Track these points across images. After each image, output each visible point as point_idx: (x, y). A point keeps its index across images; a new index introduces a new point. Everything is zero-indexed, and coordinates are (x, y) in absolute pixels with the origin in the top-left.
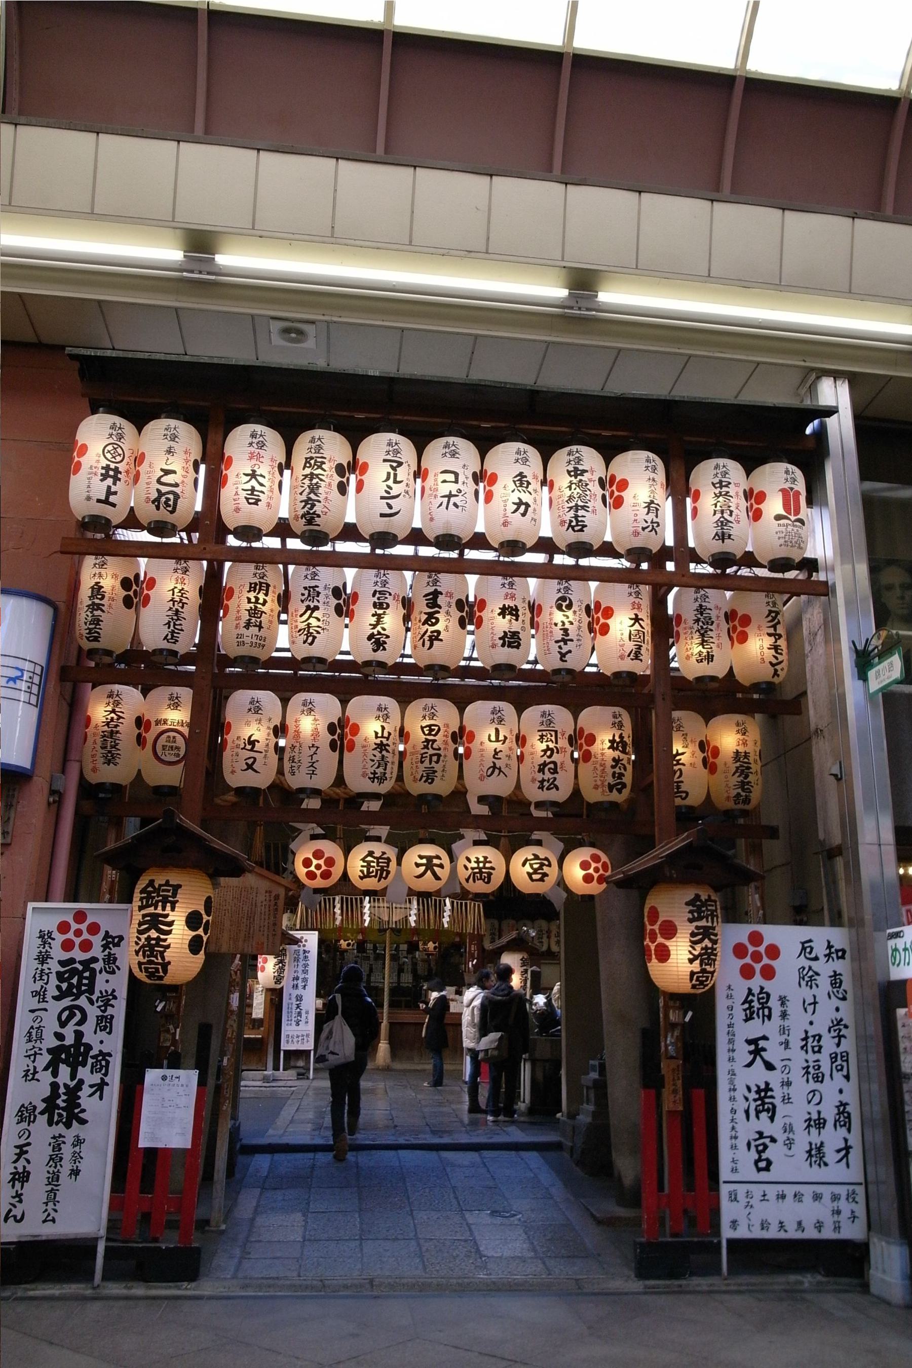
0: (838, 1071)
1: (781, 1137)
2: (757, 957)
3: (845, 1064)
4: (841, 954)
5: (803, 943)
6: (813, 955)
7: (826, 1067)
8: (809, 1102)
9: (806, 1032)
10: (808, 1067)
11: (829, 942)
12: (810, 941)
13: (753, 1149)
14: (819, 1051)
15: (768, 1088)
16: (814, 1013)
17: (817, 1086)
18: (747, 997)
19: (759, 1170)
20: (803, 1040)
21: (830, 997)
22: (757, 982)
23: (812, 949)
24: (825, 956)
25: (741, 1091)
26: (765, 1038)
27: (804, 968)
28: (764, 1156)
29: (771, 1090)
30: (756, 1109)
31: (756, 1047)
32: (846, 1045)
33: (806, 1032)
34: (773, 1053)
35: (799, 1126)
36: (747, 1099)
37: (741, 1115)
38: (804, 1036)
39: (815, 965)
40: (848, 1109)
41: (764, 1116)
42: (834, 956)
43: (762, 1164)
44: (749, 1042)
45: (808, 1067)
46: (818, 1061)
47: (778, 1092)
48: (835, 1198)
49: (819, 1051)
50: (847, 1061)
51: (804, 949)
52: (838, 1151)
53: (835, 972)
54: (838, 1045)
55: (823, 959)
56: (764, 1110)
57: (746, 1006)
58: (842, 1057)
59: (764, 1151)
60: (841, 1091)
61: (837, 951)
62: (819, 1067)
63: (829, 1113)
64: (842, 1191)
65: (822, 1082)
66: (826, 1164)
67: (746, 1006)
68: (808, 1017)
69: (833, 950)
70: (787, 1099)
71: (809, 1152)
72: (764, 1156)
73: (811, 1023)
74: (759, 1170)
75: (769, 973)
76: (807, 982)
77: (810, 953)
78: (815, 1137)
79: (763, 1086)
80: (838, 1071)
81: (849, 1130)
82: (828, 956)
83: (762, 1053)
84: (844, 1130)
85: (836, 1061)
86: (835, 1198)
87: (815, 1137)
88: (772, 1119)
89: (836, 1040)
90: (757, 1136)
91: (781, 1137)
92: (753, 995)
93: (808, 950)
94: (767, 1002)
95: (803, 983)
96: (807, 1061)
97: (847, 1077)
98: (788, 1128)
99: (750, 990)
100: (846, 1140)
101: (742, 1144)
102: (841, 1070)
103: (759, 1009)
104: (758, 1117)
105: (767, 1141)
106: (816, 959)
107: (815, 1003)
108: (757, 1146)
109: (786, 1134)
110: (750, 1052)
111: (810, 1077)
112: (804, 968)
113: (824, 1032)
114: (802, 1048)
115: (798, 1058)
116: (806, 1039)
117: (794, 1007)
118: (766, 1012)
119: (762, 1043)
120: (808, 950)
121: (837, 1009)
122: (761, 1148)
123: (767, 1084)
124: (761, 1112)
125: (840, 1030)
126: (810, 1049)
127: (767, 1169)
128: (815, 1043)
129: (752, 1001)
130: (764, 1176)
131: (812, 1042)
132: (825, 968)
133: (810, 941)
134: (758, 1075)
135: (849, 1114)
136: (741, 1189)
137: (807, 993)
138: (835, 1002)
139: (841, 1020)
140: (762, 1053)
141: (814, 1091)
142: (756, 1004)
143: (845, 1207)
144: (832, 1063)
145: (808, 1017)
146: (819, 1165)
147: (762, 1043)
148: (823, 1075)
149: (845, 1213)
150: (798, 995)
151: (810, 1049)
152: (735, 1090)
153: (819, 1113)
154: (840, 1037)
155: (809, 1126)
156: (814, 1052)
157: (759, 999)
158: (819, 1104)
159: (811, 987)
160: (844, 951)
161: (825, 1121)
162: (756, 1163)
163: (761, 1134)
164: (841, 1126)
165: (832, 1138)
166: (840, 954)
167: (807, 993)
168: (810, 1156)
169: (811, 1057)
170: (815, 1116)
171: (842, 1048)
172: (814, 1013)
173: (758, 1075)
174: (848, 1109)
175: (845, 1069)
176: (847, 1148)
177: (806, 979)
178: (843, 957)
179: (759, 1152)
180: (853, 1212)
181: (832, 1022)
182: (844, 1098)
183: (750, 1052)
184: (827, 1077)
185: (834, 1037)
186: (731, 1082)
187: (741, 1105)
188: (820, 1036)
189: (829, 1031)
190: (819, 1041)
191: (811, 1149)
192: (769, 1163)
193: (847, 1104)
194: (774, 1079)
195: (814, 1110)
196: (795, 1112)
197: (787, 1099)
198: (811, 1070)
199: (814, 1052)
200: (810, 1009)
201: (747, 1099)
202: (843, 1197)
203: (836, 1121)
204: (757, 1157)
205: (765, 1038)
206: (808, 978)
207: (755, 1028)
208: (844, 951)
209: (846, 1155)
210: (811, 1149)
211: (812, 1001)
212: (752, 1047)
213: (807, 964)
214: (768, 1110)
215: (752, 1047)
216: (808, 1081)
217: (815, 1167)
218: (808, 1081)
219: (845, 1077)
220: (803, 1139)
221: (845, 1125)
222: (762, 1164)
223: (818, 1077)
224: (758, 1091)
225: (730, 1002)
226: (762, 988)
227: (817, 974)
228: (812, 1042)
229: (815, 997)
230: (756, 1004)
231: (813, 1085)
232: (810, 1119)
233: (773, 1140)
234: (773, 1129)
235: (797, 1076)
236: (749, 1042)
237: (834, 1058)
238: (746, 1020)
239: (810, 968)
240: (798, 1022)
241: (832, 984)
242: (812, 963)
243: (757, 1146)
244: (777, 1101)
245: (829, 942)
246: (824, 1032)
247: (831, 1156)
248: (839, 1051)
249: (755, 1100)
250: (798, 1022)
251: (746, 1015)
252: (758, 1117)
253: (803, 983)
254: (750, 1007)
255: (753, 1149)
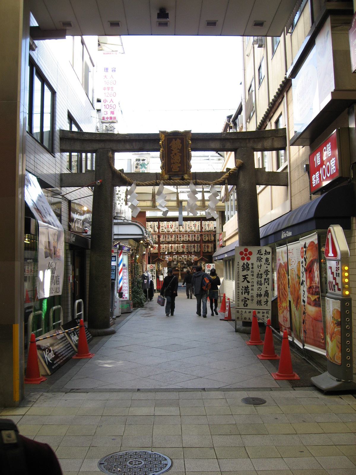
0: (266, 283)
1: (250, 298)
2: (246, 255)
3: (268, 281)
4: (269, 253)
5: (258, 251)
6: (261, 254)
7: (263, 282)
8: (258, 290)
9: (258, 273)
10: (258, 282)
11: (266, 250)
12: (261, 250)
13: (243, 301)
14: (261, 278)
15: (248, 287)
16: (260, 268)
17: (260, 286)
18: (243, 265)
19: (245, 306)
20: (257, 275)
21: (265, 264)
22: (245, 261)
23: (261, 252)
24: (264, 254)
25: (241, 287)
26: (247, 275)
27: (258, 257)
28: (246, 303)
29: (249, 288)
30: (244, 292)
31: (245, 277)
32: (268, 276)
33: (258, 273)
34: (249, 278)
35: (255, 296)
36: (242, 290)
37: (240, 293)
38: (257, 274)
39: (261, 256)
40: (268, 292)
41: (246, 294)
42: (267, 254)
43: (245, 305)
44: (243, 276)
45: (258, 282)
46: (261, 280)
47: (250, 288)
48: (263, 313)
49: (261, 278)
50: (269, 280)
51: (259, 252)
52: (265, 302)
53: (267, 258)
54: (267, 276)
55: (264, 255)
56: (246, 292)
57: (243, 267)
58: (267, 279)
59: (246, 302)
60: (266, 288)
61: (268, 252)
62: (261, 282)
63: (263, 293)
64: (265, 311)
65: (262, 285)
66: (262, 305)
67: (243, 267)
68: (259, 269)
69: (267, 252)
70: (252, 290)
71: (257, 302)
72: (246, 303)
73: (260, 271)
74: (245, 306)
75: (249, 259)
76: (259, 261)
77: (260, 253)
78: (259, 299)
79: (246, 287)
80: (266, 283)
81: (268, 297)
82: (265, 254)
83: (247, 279)
84: (267, 297)
85: (266, 280)
86: (263, 313)
87: (259, 299)
88: (248, 295)
89: (266, 275)
90: (244, 298)
91: (250, 298)
92: (245, 265)
93: (260, 252)
94: (248, 266)
95: (258, 261)
96: (258, 280)
97: (268, 284)
98: (252, 296)
99: (244, 263)
100: (267, 299)
101: (240, 300)
102: (267, 282)
103: (246, 268)
104: (245, 294)
105: (247, 300)
106: (262, 254)
107: (261, 266)
108: (244, 301)
109: (252, 298)
110: (243, 278)
111: (259, 284)
112: (258, 257)
113: (263, 273)
114: (257, 277)
115: (256, 280)
116: (258, 275)
117: (255, 266)
118: (248, 268)
119: (246, 276)
120: (260, 252)
121: (267, 267)
122: (245, 301)
123: (247, 286)
124: (246, 293)
125: (267, 272)
126: (259, 277)
127: (247, 306)
128: (261, 276)
129: (245, 266)
130: (246, 307)
131: (259, 276)
132: (264, 257)
133: (261, 250)
134: (245, 284)
135: (268, 293)
136: (240, 310)
137: (259, 263)
138: (266, 265)
139: (268, 270)
140: (247, 279)
141: (259, 288)
142: (245, 267)
143: (266, 315)
144: (265, 281)
145: (259, 269)
146: (260, 305)
147: (246, 276)
148: (262, 284)
149: (266, 316)
150: (256, 264)
151: (259, 277)
152: (239, 287)
153: (260, 293)
154: (267, 274)
155: (257, 296)
156: (260, 278)
157: (246, 265)
158: (260, 291)
159: (260, 262)
160: (270, 252)
161: (262, 295)
162: (244, 304)
163: (245, 298)
164: (266, 296)
165: (263, 299)
166: (269, 253)
167: (259, 263)
168: (258, 303)
169: (259, 279)
170: (259, 294)
171: (268, 277)
172: (260, 268)
173: (245, 284)
174: (268, 292)
175: (268, 282)
176: (267, 301)
177: (259, 260)
178: (269, 254)
179: (245, 302)
180: (267, 316)
181: (265, 270)
182: (267, 289)
183: (243, 278)
184: (263, 284)
185: (265, 274)
186: (238, 285)
187: (240, 291)
188: (262, 274)
189: (264, 273)
190: (261, 275)
191: (258, 301)
192: (247, 305)
193: (268, 291)
194: (249, 285)
195: (259, 292)
196: (254, 292)
197: (252, 290)
198: (259, 283)
199: (260, 278)
200: (260, 267)
201: (242, 290)
202: (265, 313)
203: (264, 295)
204: (244, 303)
205: (247, 275)
206: (259, 259)
207: (245, 273)
208: (270, 252)
209: (267, 303)
210: (258, 301)
211: (260, 265)
212: (244, 277)
213: (259, 256)
214: (247, 292)
215: (244, 277)
216: (258, 285)
217: (259, 306)
218: (258, 285)
219: (268, 284)
220: (256, 299)
221: (267, 296)
222: (245, 305)
223: (261, 284)
224: (245, 288)
225: (238, 266)
226: (247, 263)
227: (262, 258)
228: (259, 276)
229: (261, 264)
230: (245, 267)
231: (259, 286)
232: (258, 294)
233: (248, 299)
234: (249, 297)
235: (255, 284)
236: (243, 276)
237: (265, 279)
238: (243, 271)
239: (260, 257)
240: (256, 270)
241: (266, 261)
242: (260, 256)
243: (244, 301)
244: (250, 290)
245: (266, 250)
246: (263, 273)
247: (263, 303)
248: (266, 278)
249: (244, 290)
250: (256, 270)
251: (243, 269)
252: (245, 294)
253: (258, 261)
254: (244, 267)
255: (243, 301)
